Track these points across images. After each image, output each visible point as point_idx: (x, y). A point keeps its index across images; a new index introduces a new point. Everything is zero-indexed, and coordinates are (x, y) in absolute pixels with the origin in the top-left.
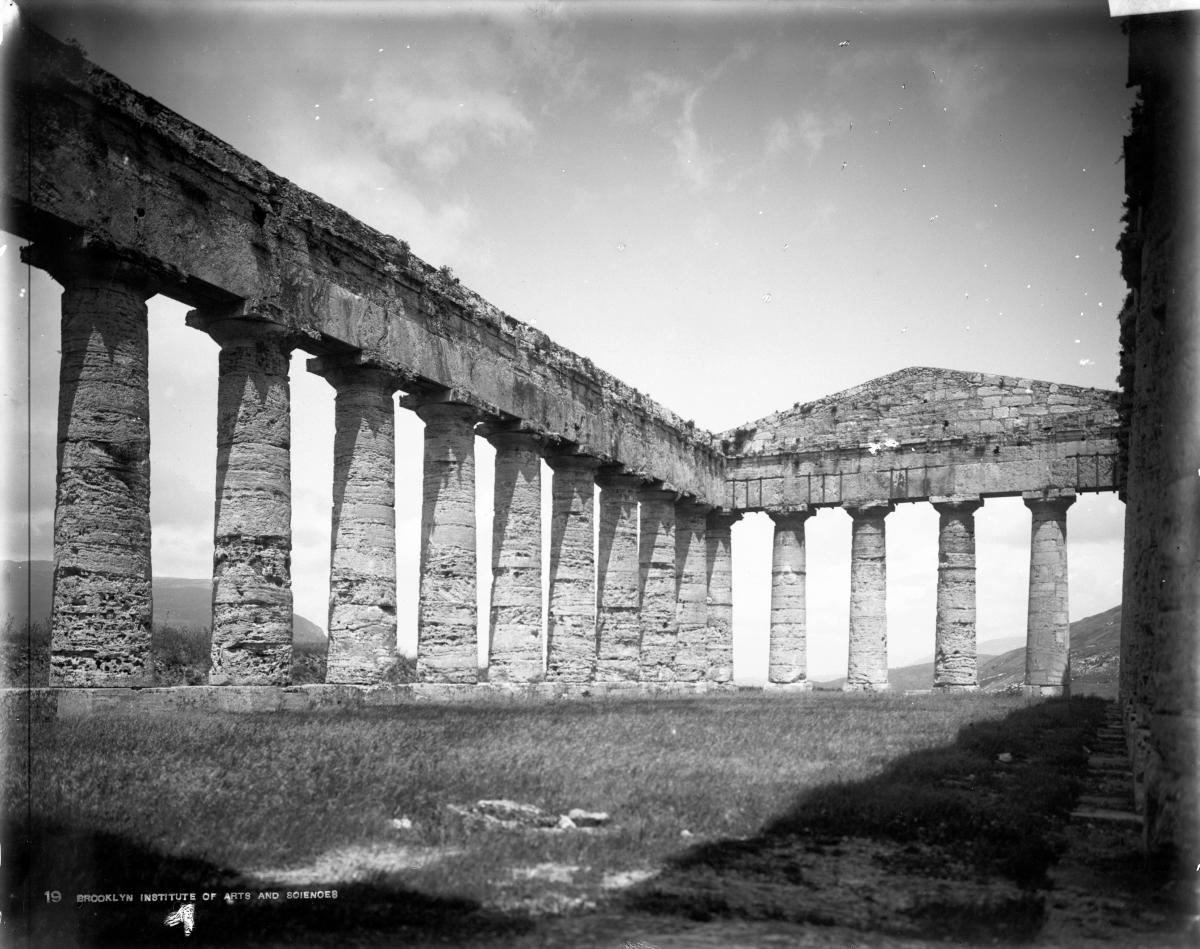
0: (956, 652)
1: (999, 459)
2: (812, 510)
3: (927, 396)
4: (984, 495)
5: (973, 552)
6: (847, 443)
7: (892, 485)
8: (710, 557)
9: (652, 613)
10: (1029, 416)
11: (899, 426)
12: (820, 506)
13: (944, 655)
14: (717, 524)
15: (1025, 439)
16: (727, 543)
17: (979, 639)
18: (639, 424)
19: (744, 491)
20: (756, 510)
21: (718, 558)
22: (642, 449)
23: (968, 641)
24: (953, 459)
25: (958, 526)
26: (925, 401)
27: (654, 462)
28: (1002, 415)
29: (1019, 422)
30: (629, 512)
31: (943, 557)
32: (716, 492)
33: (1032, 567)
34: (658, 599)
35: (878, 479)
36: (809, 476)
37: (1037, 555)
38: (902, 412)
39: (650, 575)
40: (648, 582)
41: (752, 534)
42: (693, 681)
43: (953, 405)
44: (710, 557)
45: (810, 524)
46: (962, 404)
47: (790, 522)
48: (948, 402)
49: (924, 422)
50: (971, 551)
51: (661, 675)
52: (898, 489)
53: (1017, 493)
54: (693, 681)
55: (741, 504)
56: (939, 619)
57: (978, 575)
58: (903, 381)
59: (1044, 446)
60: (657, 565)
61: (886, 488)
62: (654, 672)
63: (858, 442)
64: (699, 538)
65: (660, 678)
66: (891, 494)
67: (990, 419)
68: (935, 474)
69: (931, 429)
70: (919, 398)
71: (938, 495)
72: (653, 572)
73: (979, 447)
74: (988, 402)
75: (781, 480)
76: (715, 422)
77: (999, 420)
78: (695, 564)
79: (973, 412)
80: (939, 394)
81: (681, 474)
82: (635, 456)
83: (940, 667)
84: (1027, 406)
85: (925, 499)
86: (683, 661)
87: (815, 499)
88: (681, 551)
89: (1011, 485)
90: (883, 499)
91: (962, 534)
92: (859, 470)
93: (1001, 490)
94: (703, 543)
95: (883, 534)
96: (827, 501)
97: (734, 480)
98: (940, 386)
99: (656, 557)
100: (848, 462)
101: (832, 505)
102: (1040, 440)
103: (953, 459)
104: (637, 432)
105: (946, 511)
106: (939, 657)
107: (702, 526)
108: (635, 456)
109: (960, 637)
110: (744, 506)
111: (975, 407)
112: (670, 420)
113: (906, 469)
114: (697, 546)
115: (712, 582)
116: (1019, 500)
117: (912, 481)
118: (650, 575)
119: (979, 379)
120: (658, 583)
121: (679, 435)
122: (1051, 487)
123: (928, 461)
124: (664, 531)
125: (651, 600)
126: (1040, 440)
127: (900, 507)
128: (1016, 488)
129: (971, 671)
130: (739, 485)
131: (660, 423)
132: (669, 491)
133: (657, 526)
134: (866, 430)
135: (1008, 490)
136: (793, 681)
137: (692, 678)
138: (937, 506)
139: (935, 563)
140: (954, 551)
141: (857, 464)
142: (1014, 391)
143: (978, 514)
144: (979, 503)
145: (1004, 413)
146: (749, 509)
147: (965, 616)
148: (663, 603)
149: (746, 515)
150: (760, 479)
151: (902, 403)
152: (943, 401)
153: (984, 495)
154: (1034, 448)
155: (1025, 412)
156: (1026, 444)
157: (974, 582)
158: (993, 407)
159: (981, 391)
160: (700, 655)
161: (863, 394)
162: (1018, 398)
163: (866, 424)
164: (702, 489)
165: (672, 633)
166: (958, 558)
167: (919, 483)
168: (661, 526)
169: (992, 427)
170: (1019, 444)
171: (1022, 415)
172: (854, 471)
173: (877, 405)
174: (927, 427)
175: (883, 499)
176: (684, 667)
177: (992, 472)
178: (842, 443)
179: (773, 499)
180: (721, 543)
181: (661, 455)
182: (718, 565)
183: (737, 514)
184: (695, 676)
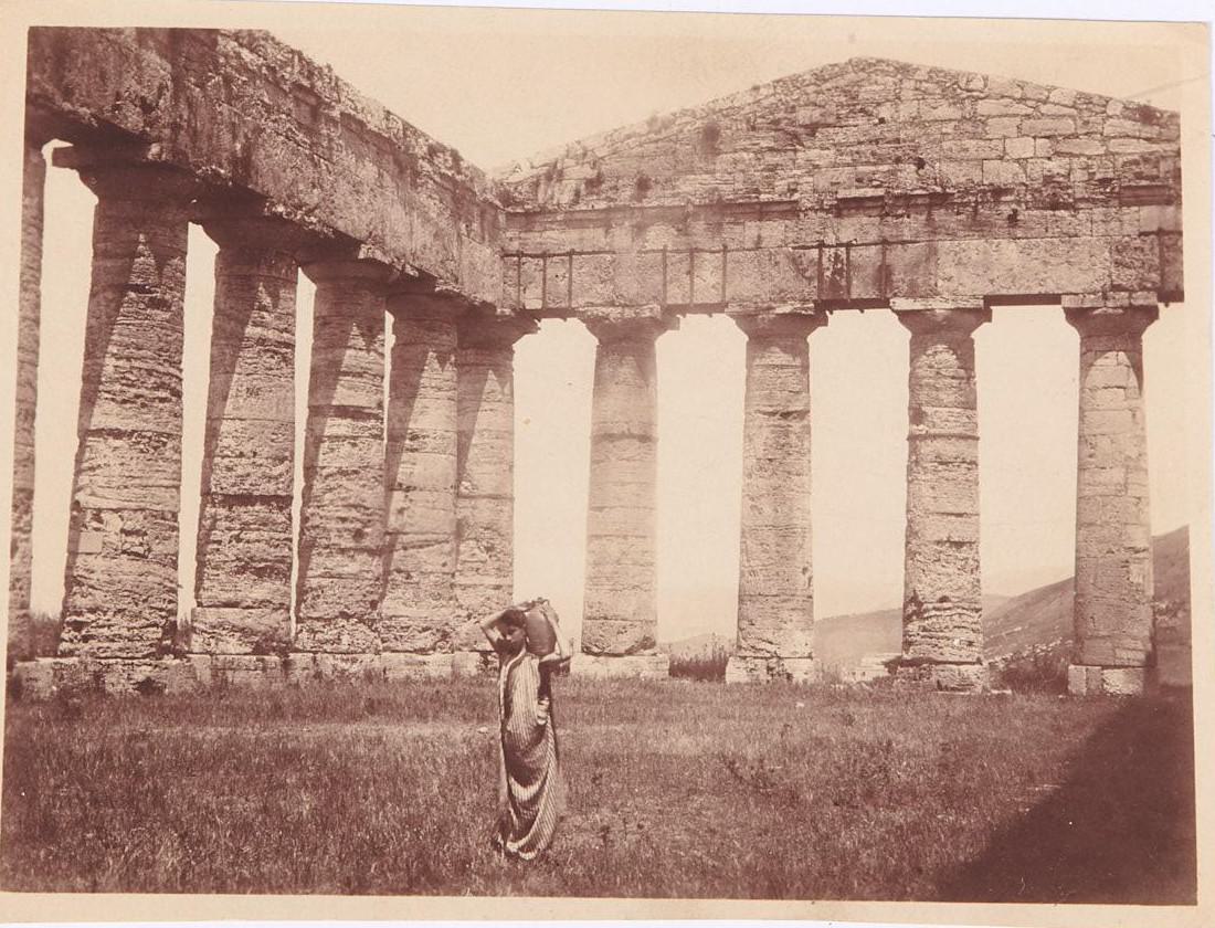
0: (944, 599)
1: (1019, 233)
2: (668, 317)
3: (885, 112)
4: (994, 300)
5: (973, 408)
6: (735, 192)
7: (821, 274)
8: (466, 405)
9: (331, 511)
10: (1071, 155)
11: (835, 165)
12: (684, 309)
13: (920, 604)
14: (479, 336)
15: (1064, 198)
16: (504, 373)
17: (986, 573)
18: (307, 122)
19: (539, 276)
20: (563, 314)
21: (484, 405)
22: (309, 171)
23: (965, 580)
24: (933, 229)
25: (945, 357)
26: (882, 121)
27: (339, 200)
28: (1018, 157)
29: (1056, 166)
30: (275, 297)
31: (917, 416)
32: (479, 272)
33: (1082, 439)
34: (344, 482)
35: (795, 261)
36: (664, 251)
37: (1091, 416)
38: (840, 138)
39: (327, 432)
40: (325, 446)
41: (552, 360)
42: (422, 651)
43: (933, 129)
44: (466, 405)
45: (664, 343)
46: (949, 128)
47: (625, 342)
48: (923, 124)
49: (881, 160)
50: (970, 405)
51: (345, 639)
52: (834, 284)
53: (1053, 299)
54: (422, 651)
55: (533, 303)
56: (911, 533)
57: (984, 452)
58: (842, 82)
59: (1098, 212)
60: (343, 412)
61: (810, 279)
62: (330, 634)
63: (757, 191)
64: (442, 360)
65: (344, 648)
66: (820, 289)
67: (1001, 158)
68: (899, 257)
69: (893, 173)
70: (870, 115)
71: (906, 296)
72: (336, 426)
73: (980, 208)
74: (995, 128)
75: (608, 257)
76: (498, 149)
77: (1017, 161)
78: (432, 414)
79: (971, 144)
80: (906, 110)
81: (402, 229)
82: (294, 182)
83: (914, 627)
84: (1067, 137)
85: (882, 303)
86: (403, 611)
87: (675, 296)
88: (405, 388)
89: (1042, 282)
90: (804, 301)
91: (951, 372)
92: (758, 246)
93: (1022, 291)
94: (450, 372)
95: (805, 368)
96: (698, 300)
97: (520, 254)
98: (907, 94)
99: (343, 395)
100: (738, 229)
101: (709, 309)
102: (1094, 201)
103: (933, 229)
104: (300, 136)
105: (923, 328)
106: (912, 608)
107: (449, 339)
108: (294, 182)
109: (951, 569)
110: (541, 302)
111: (974, 136)
112: (374, 123)
113: (849, 246)
114: (437, 377)
115: (472, 453)
116: (1056, 313)
117: (858, 268)
118: (327, 432)
119: (980, 85)
120: (346, 448)
121: (398, 153)
122: (1116, 288)
123: (888, 232)
124: (361, 342)
125: (331, 482)
126: (1094, 201)
127: (837, 317)
128: (1051, 288)
129: (972, 636)
130: (530, 265)
131: (353, 126)
132: (371, 262)
133: (346, 333)
134: (773, 168)
135: (1035, 291)
136: (629, 652)
137: (419, 644)
138: (904, 316)
139: (905, 427)
140: (939, 403)
141: (755, 232)
142: (1044, 109)
143: (982, 336)
144: (983, 314)
145: (1022, 147)
146: (547, 312)
147: (958, 530)
148: (353, 489)
149: (545, 323)
150: (571, 254)
151: (839, 123)
152: (915, 121)
153: (994, 300)
154: (1081, 215)
155: (1063, 148)
156: (1066, 206)
157: (974, 463)
158: (1005, 137)
159: (984, 107)
160: (438, 597)
161: (765, 103)
162: (1050, 123)
163: (771, 159)
164: (451, 265)
165: (371, 552)
166: (943, 417)
167: (870, 271)
168: (355, 331)
169: (1003, 174)
170: (1055, 206)
171: (1058, 154)
172: (749, 245)
173: (792, 123)
174: (885, 168)
175: (804, 301)
176: (404, 622)
177: (1007, 260)
178: (727, 192)
179: (591, 292)
180: (491, 375)
181: (357, 189)
182: (485, 419)
183: (526, 320)
184: (425, 640)
